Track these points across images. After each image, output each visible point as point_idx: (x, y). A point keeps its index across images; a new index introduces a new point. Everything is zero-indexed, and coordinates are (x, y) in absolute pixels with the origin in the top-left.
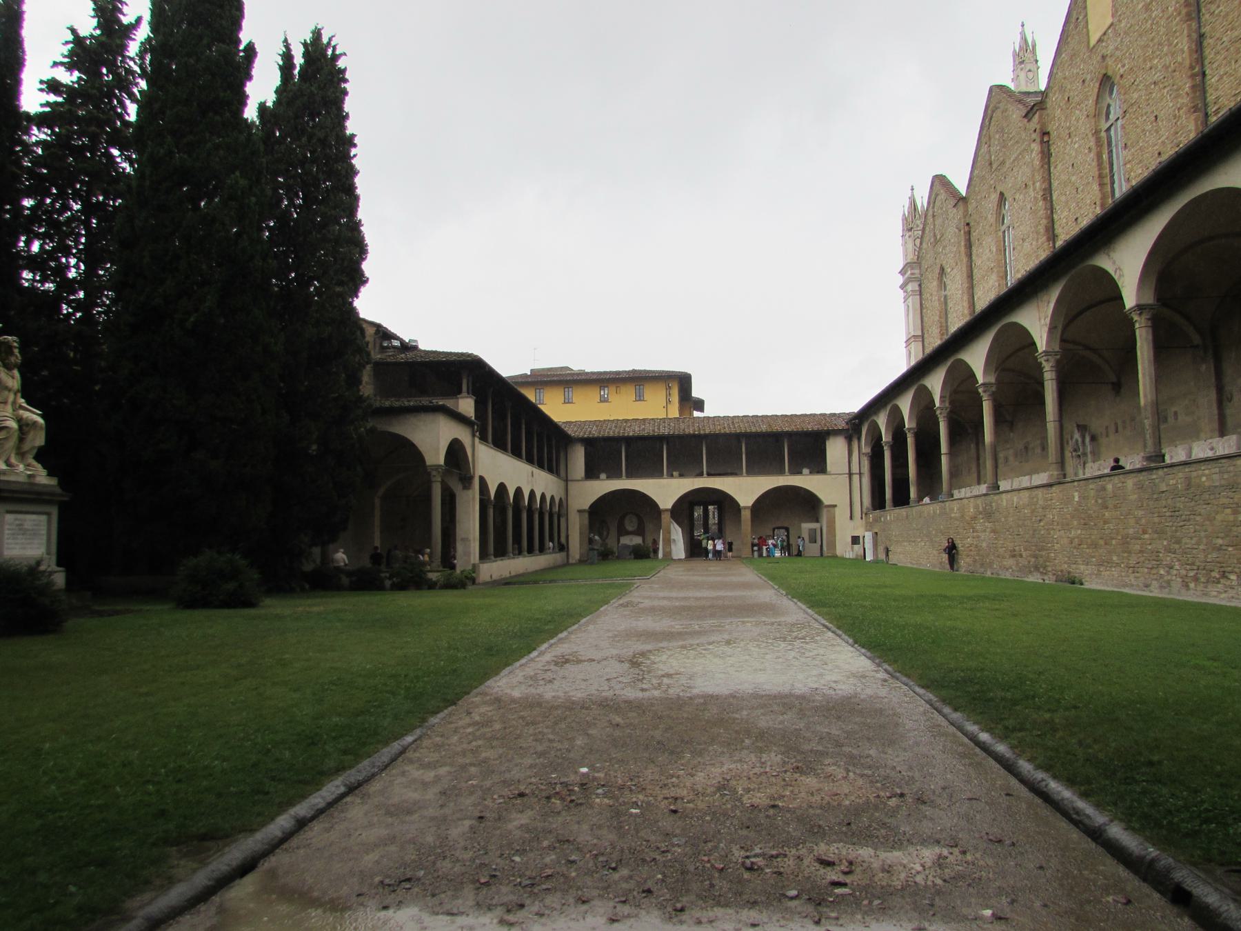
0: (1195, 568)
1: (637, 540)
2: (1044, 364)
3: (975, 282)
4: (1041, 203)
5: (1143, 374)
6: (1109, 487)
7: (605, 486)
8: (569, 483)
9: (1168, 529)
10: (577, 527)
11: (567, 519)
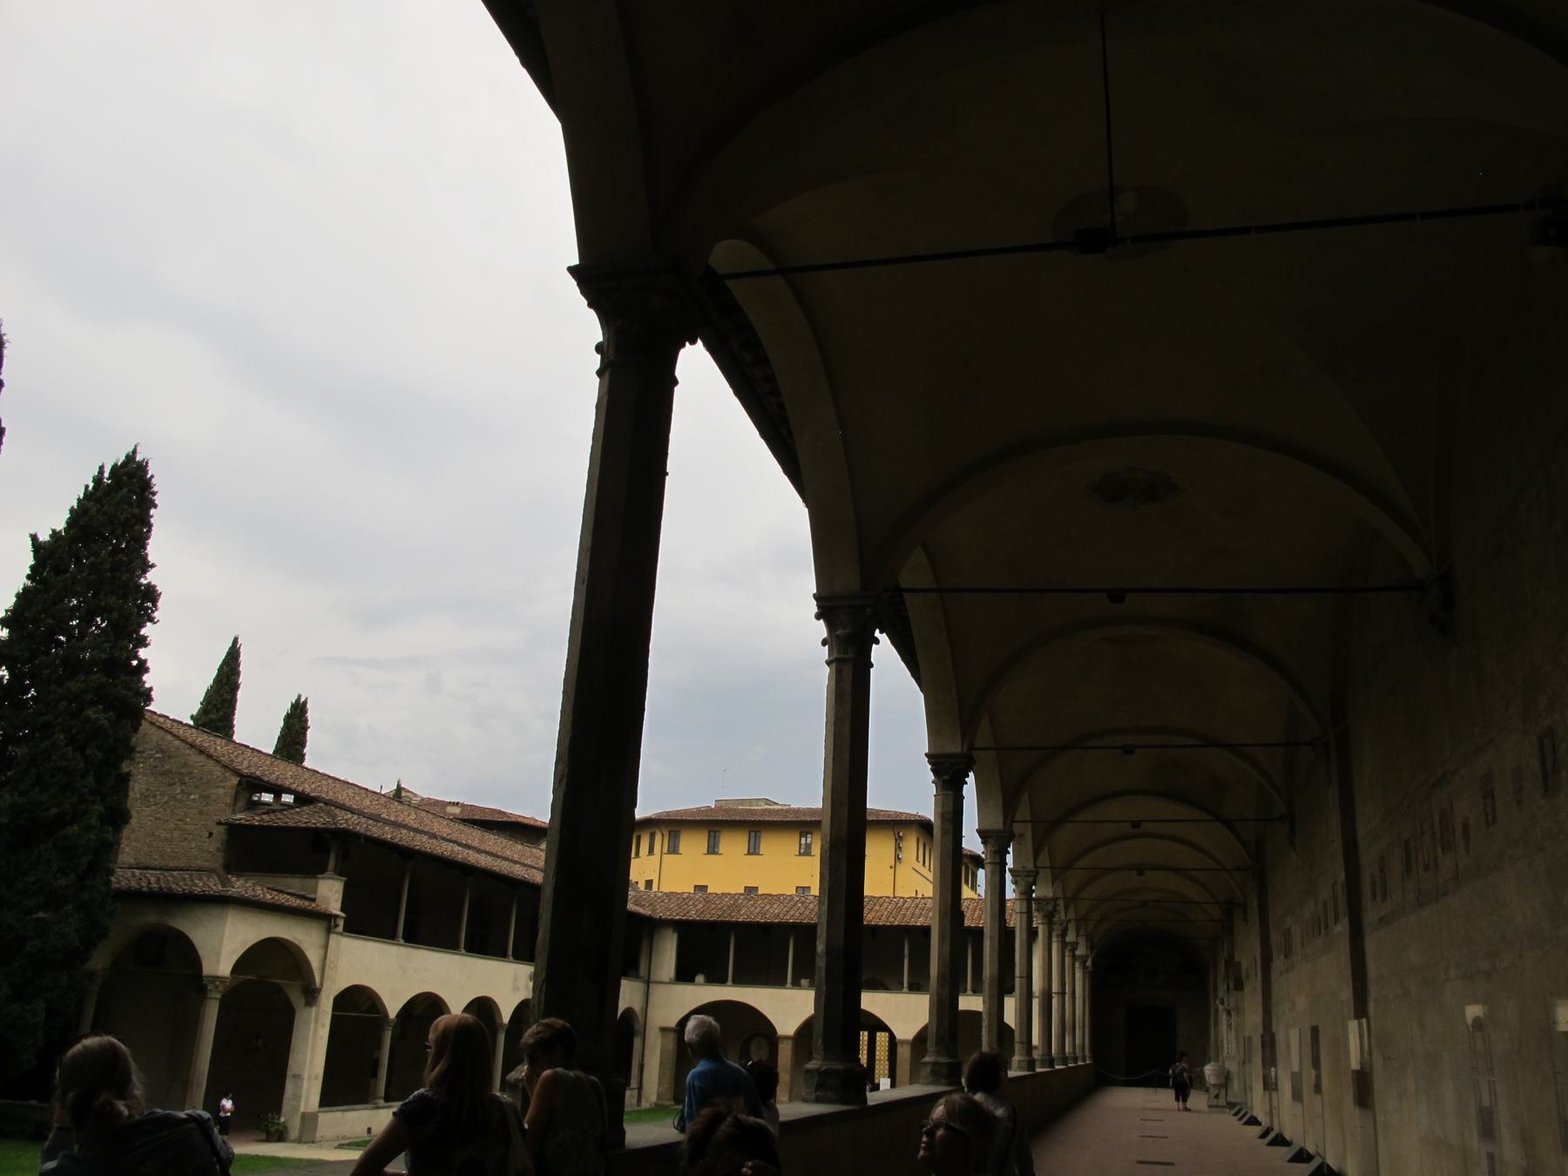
8: (651, 985)
10: (658, 1053)
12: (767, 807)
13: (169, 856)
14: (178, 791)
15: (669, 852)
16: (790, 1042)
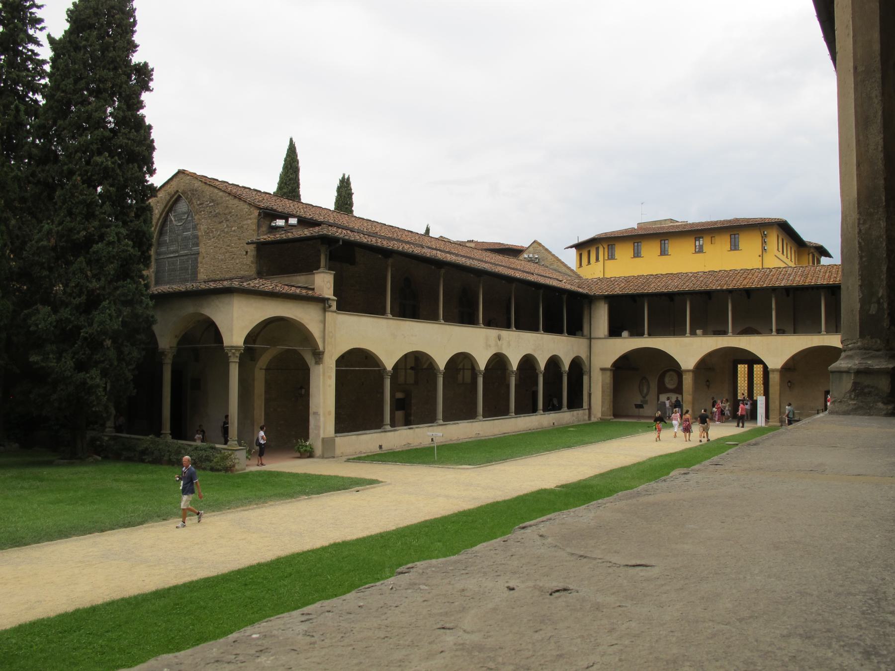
7: (627, 344)
8: (592, 340)
10: (600, 385)
12: (672, 224)
13: (225, 271)
14: (225, 226)
15: (609, 259)
16: (691, 374)
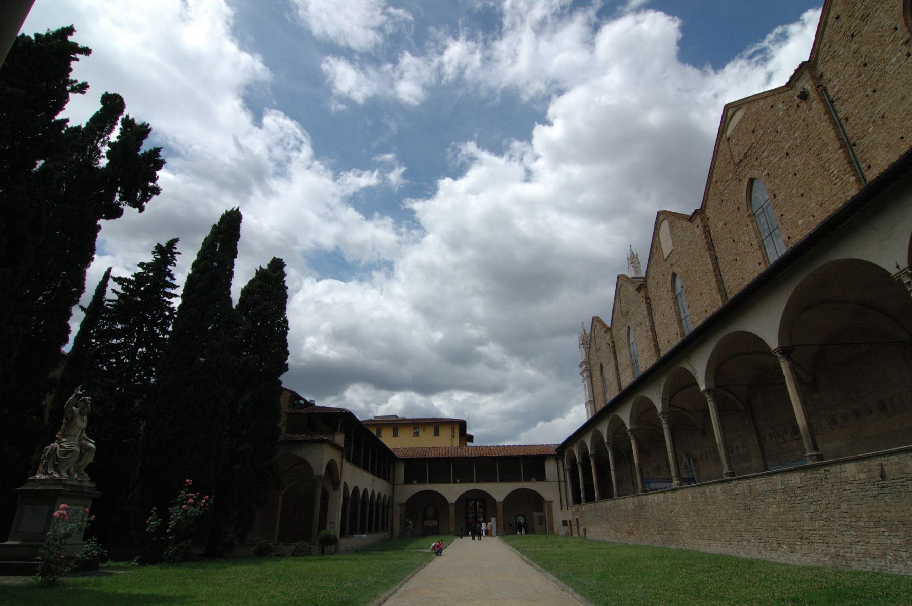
0: (763, 541)
1: (434, 523)
2: (662, 419)
3: (620, 372)
4: (650, 333)
5: (715, 426)
6: (707, 491)
8: (395, 486)
9: (744, 516)
11: (393, 509)
